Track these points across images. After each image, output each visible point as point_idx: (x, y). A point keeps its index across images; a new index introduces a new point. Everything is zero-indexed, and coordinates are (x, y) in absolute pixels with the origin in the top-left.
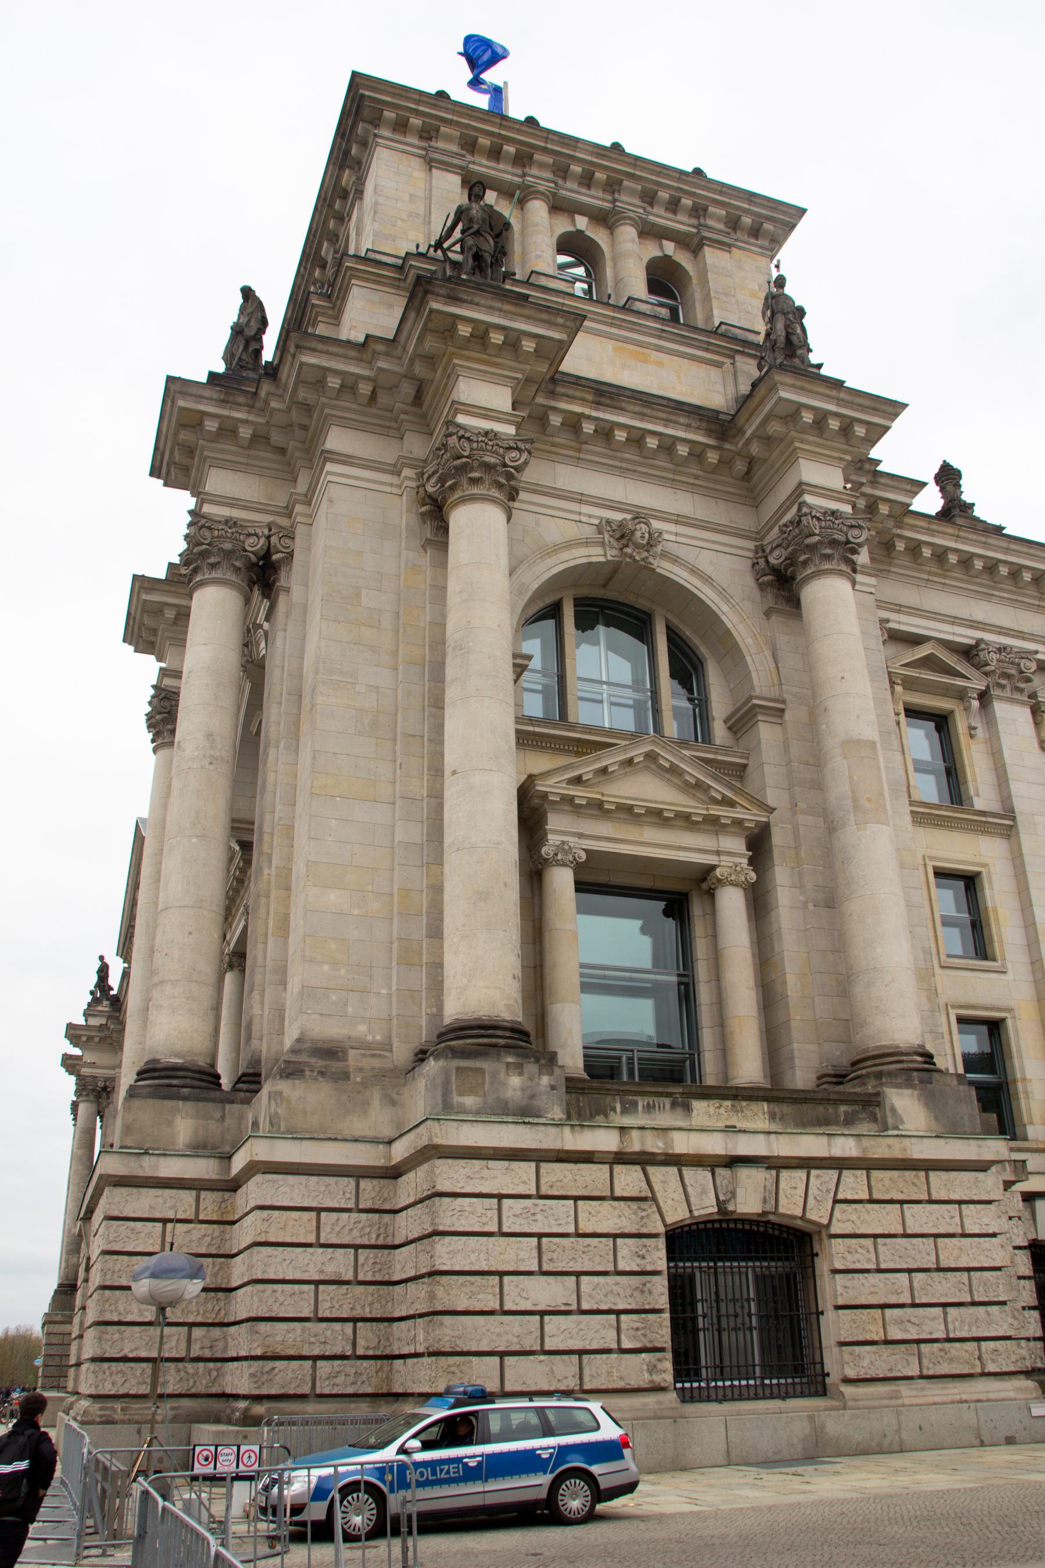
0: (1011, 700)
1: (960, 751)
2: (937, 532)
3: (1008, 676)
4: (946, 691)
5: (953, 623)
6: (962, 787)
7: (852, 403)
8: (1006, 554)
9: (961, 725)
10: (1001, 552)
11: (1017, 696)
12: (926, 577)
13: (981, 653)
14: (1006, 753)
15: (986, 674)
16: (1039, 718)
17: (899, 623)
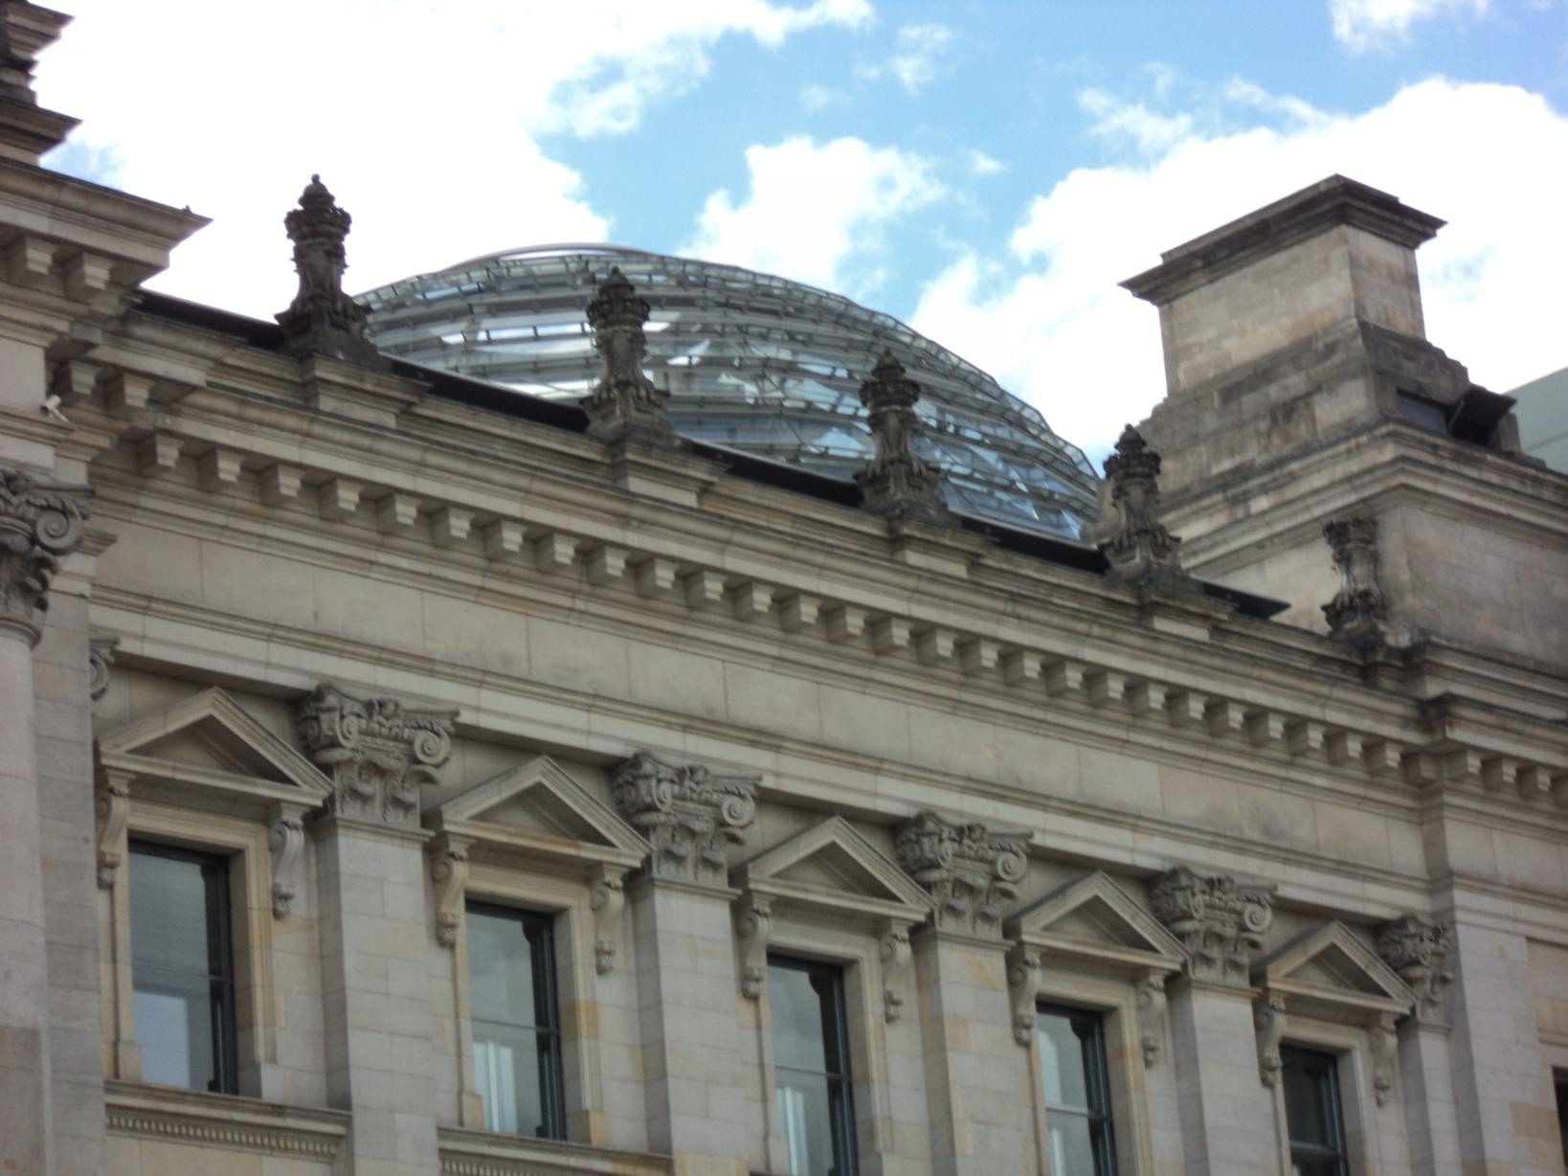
0: (379, 830)
1: (247, 950)
2: (261, 423)
3: (381, 772)
4: (231, 805)
5: (269, 638)
6: (241, 1036)
7: (86, 213)
8: (416, 474)
9: (256, 884)
10: (406, 471)
11: (396, 819)
12: (219, 519)
13: (324, 717)
14: (351, 962)
15: (327, 769)
16: (442, 870)
17: (142, 638)
